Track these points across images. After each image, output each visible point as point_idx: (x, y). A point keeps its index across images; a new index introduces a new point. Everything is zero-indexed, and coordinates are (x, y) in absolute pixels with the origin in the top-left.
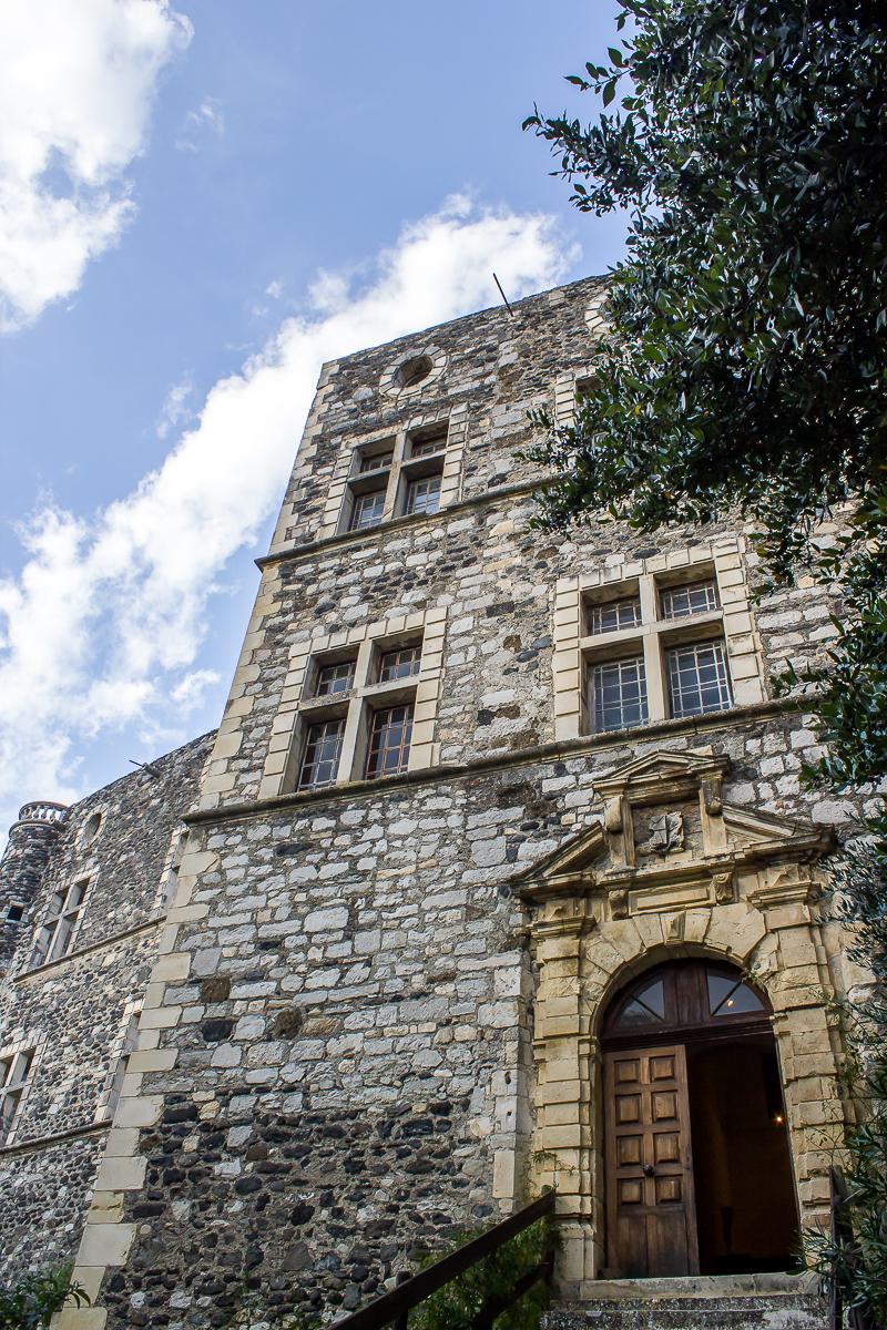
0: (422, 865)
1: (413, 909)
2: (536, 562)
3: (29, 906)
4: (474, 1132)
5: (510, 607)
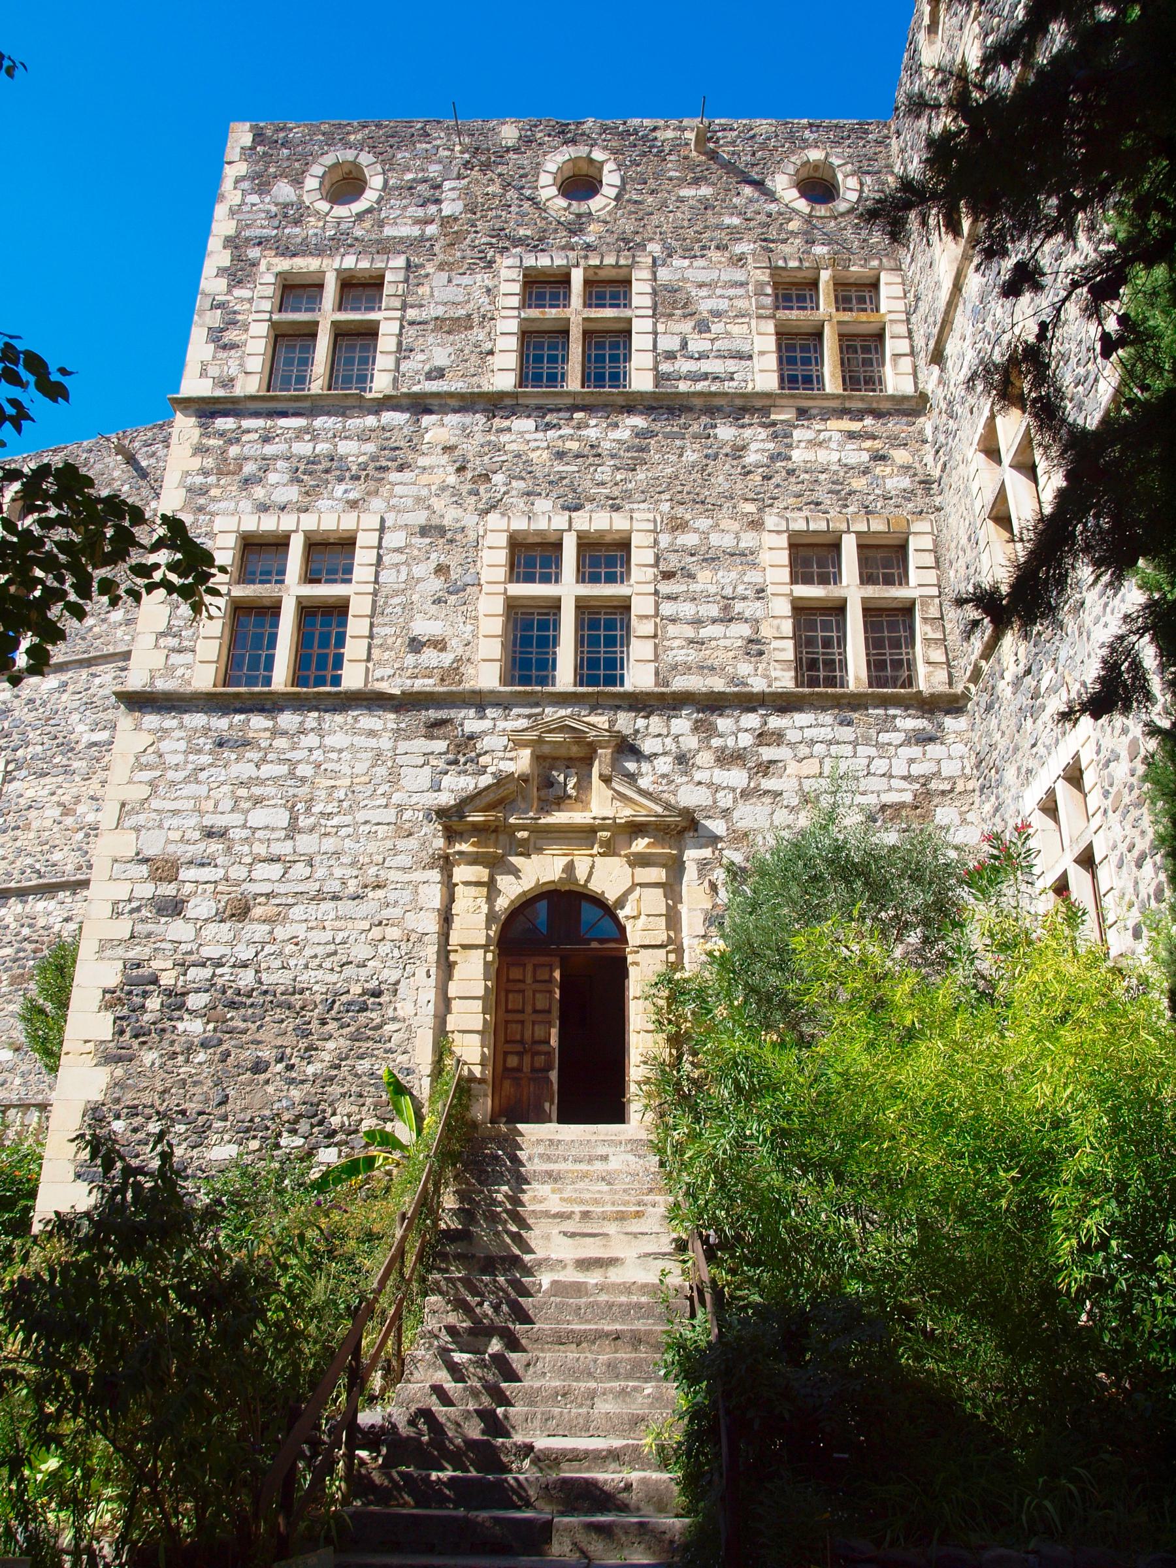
0: (356, 781)
1: (348, 819)
2: (469, 487)
4: (400, 1013)
5: (441, 531)
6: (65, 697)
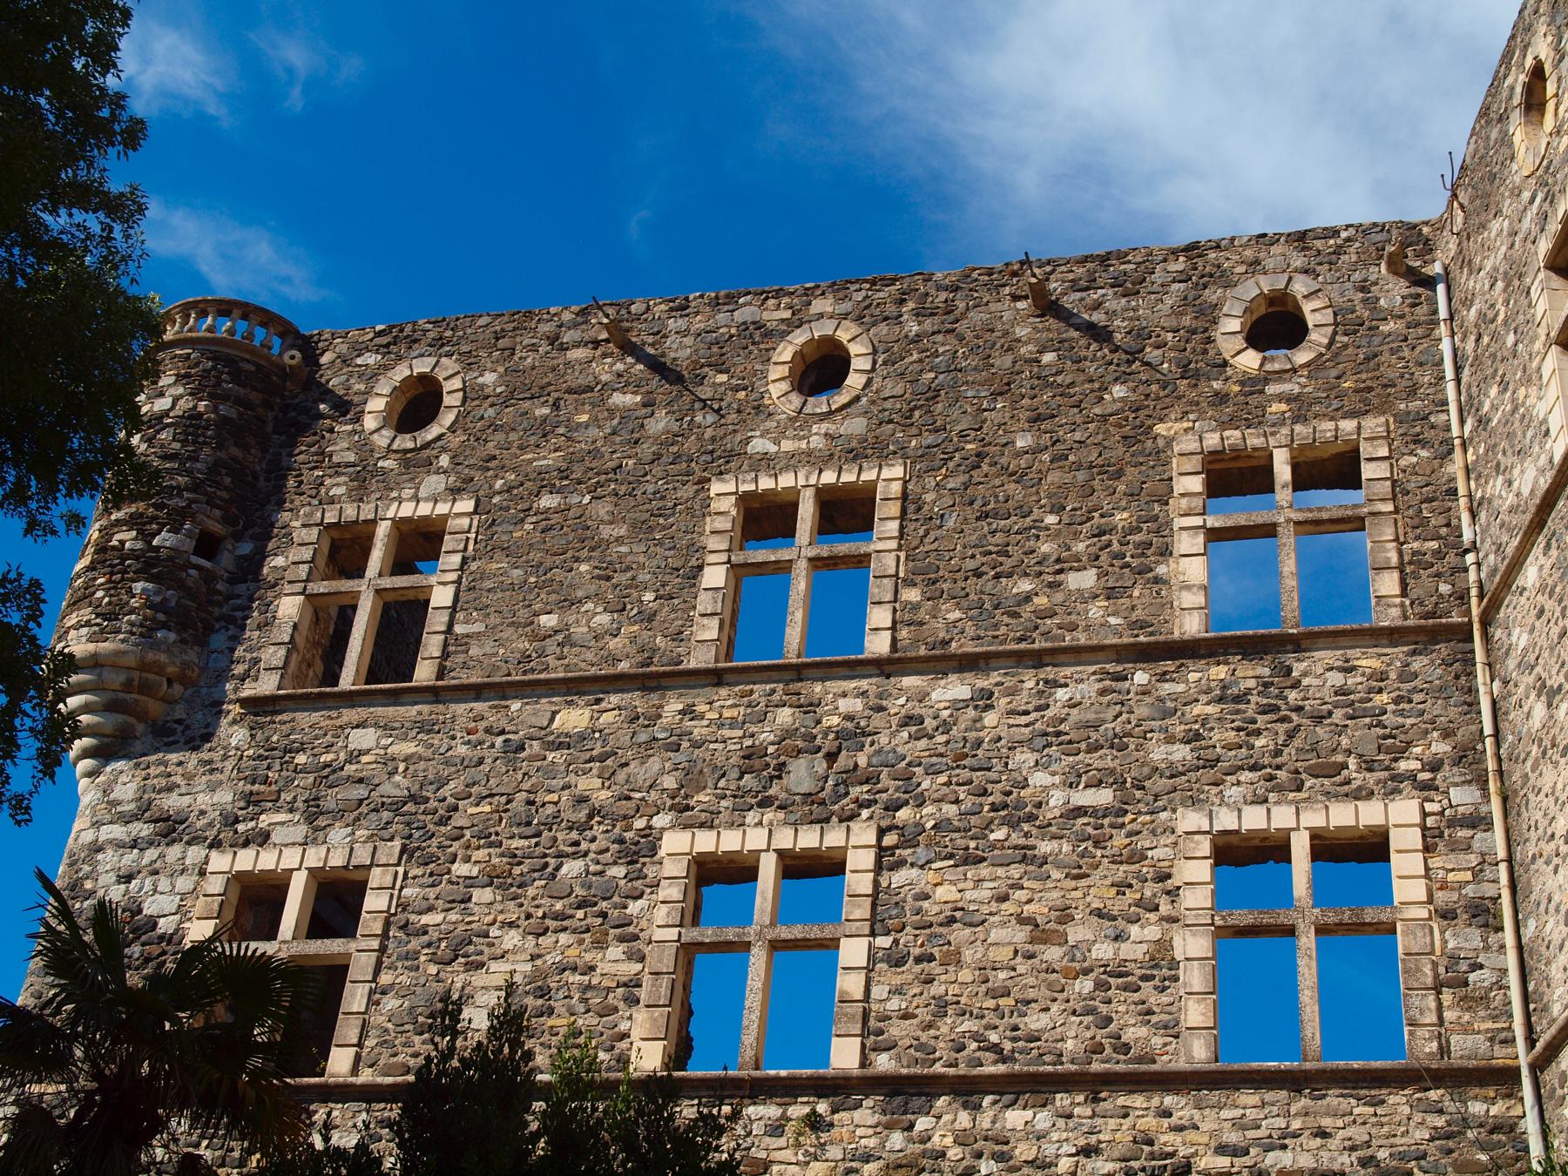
3: (238, 537)
6: (990, 719)
